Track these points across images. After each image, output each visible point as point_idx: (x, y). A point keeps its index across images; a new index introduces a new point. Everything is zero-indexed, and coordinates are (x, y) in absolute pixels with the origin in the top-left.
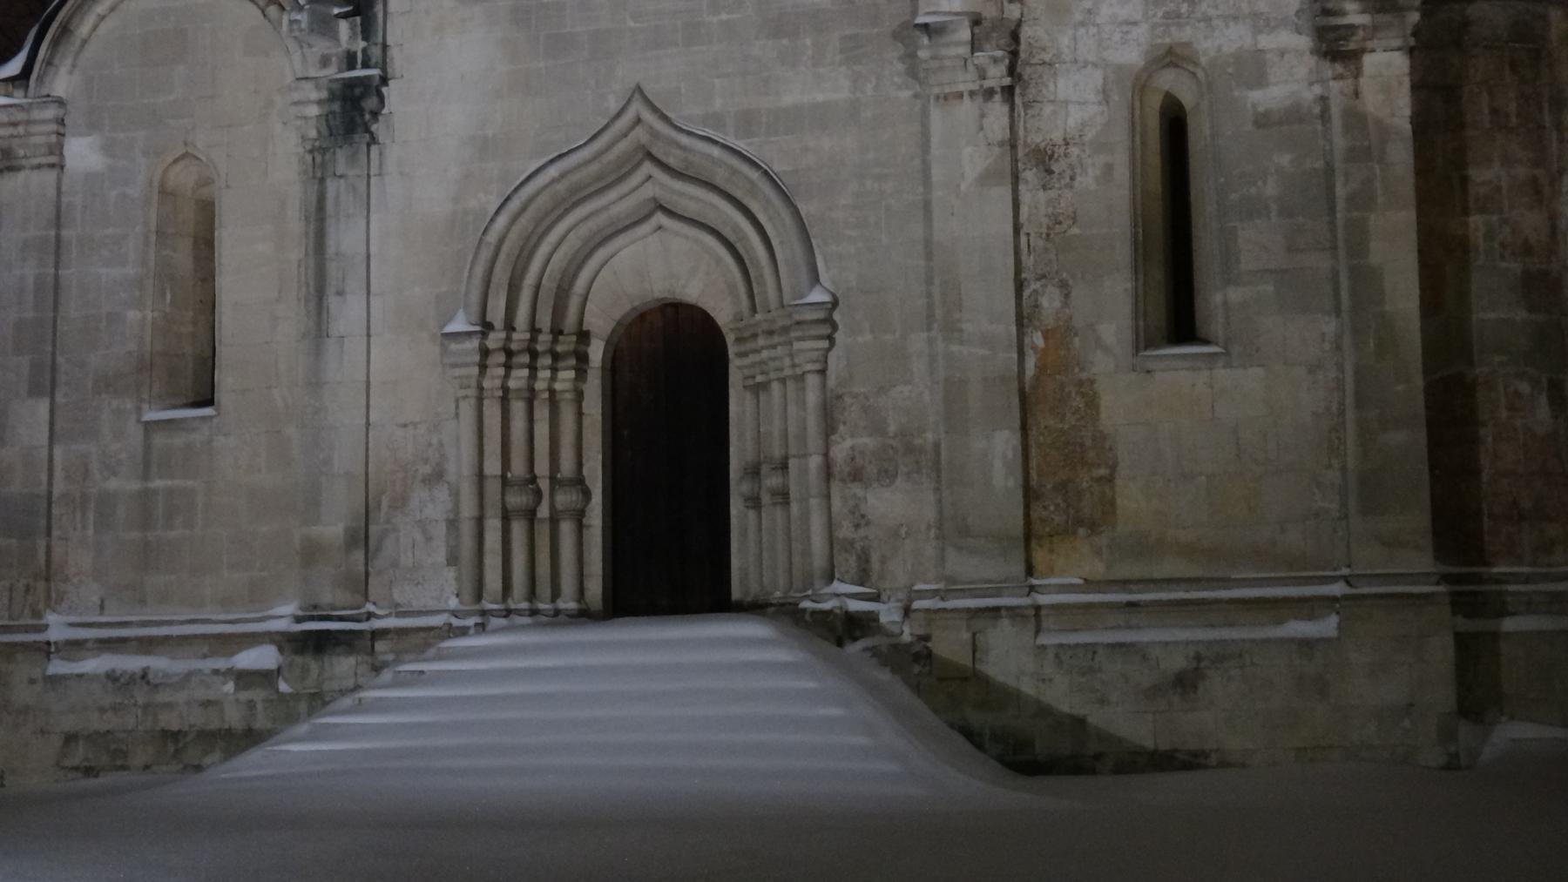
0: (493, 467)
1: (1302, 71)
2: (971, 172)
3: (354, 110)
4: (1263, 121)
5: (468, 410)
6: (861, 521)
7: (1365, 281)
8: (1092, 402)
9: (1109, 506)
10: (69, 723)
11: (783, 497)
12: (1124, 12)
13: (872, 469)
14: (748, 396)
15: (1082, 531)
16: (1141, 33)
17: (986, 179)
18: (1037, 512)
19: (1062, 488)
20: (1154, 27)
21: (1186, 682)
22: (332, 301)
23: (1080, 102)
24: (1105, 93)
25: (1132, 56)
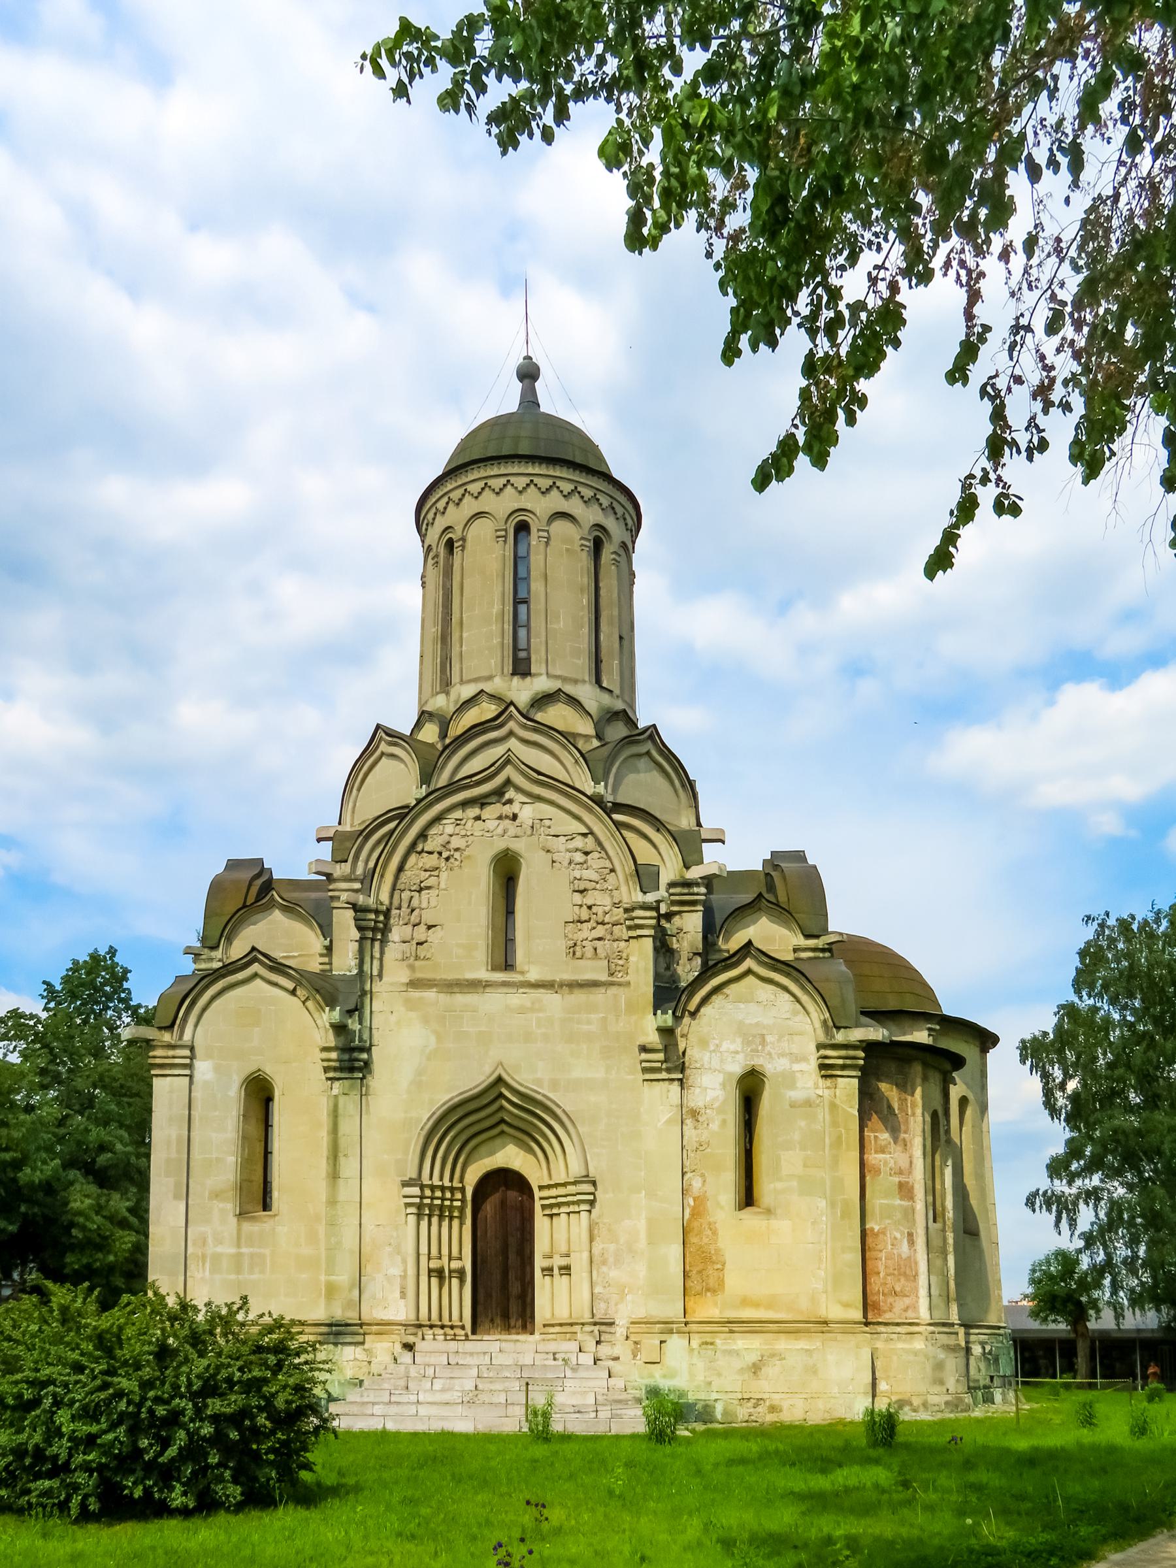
0: (424, 1249)
1: (811, 1084)
3: (352, 1060)
8: (715, 1233)
12: (732, 1047)
13: (611, 1260)
15: (709, 1294)
16: (740, 1057)
17: (669, 1121)
18: (689, 1284)
19: (700, 1272)
20: (746, 1056)
23: (714, 1088)
24: (724, 1085)
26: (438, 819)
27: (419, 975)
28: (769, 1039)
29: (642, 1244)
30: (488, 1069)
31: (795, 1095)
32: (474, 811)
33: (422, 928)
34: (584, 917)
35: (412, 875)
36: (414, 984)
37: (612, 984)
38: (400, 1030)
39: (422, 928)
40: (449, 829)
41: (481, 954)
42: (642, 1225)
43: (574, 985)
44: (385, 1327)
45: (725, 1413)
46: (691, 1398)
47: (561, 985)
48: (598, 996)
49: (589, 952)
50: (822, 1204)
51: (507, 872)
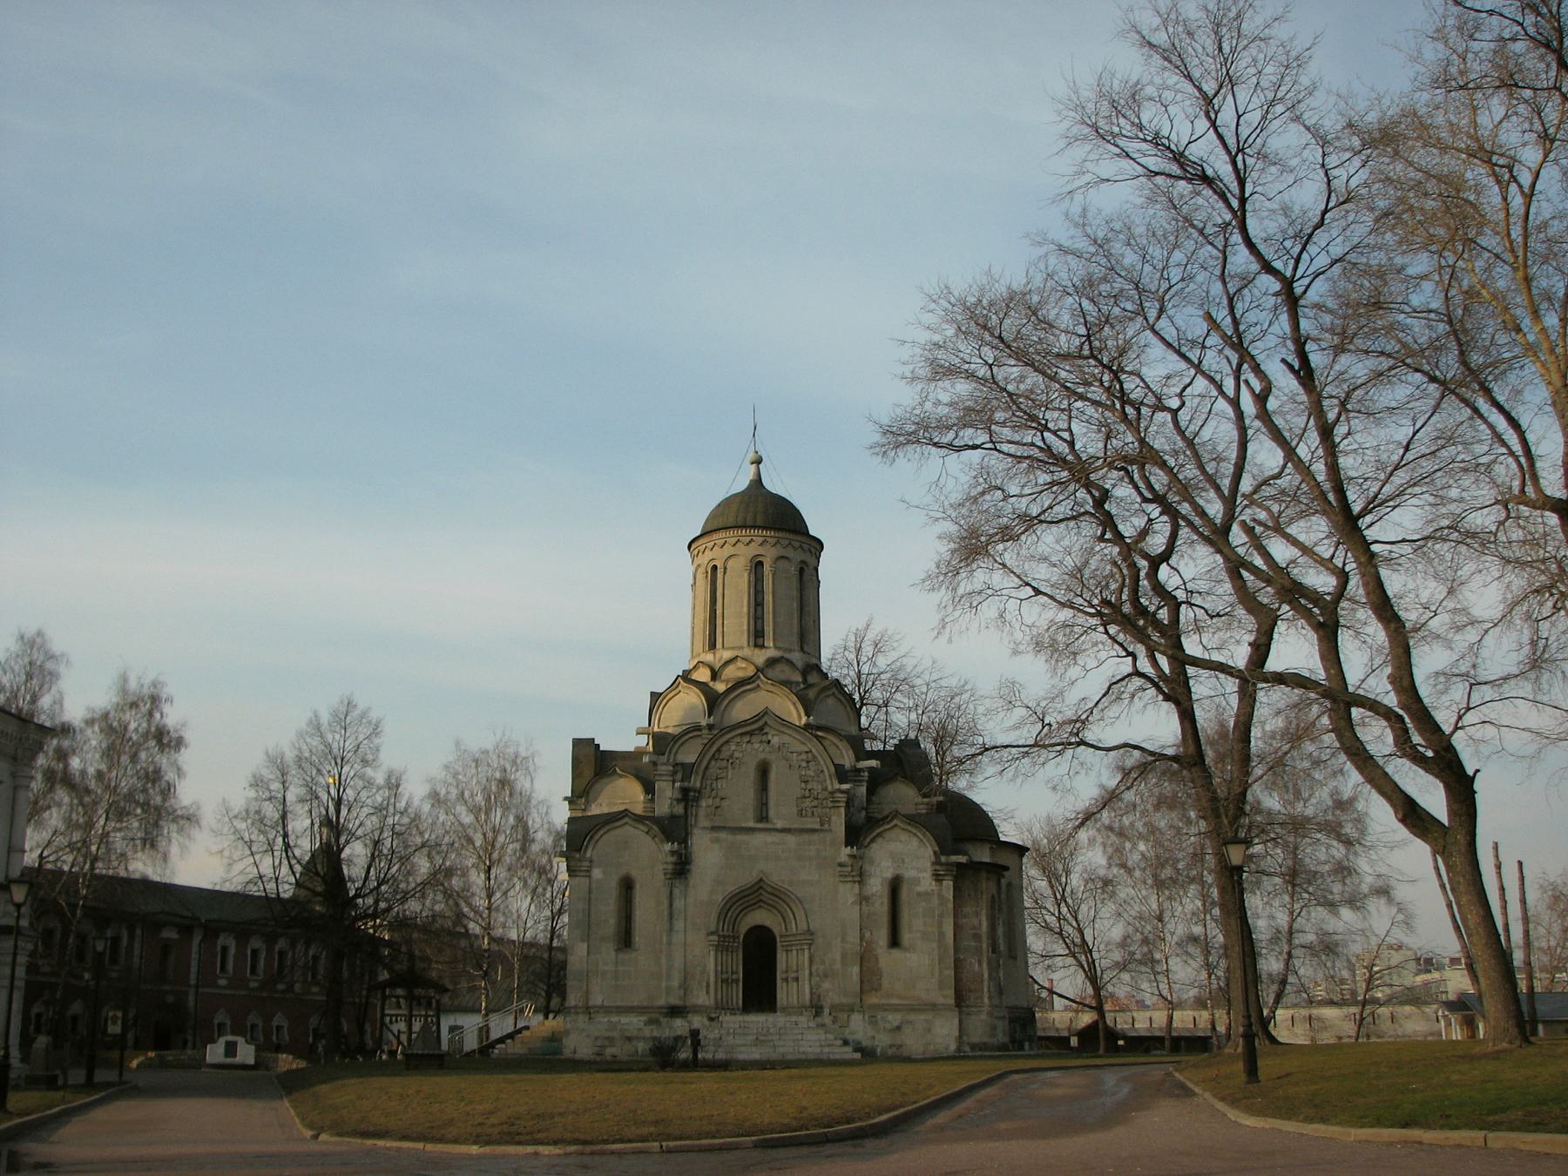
4: (919, 894)
7: (942, 935)
11: (797, 979)
21: (898, 1028)
23: (877, 885)
25: (889, 875)
29: (838, 965)
31: (919, 889)
32: (746, 739)
35: (713, 770)
36: (714, 828)
38: (707, 852)
41: (750, 814)
42: (838, 957)
43: (802, 831)
48: (815, 837)
50: (935, 945)
51: (764, 771)
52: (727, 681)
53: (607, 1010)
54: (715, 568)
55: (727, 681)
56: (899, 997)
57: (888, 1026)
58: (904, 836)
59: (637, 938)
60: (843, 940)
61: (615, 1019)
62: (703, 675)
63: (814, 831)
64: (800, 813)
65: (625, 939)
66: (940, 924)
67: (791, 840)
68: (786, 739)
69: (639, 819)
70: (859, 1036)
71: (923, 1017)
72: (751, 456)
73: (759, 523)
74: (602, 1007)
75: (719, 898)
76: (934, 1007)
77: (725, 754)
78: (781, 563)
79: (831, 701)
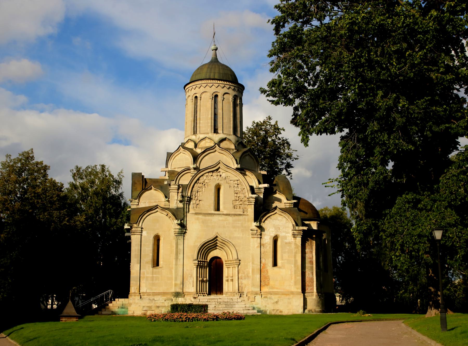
2: (256, 246)
4: (286, 243)
5: (195, 269)
6: (242, 284)
7: (296, 261)
8: (267, 272)
9: (269, 283)
10: (144, 305)
11: (232, 280)
14: (227, 269)
16: (274, 232)
17: (257, 247)
21: (277, 302)
22: (178, 254)
23: (268, 239)
24: (270, 239)
25: (273, 235)
26: (202, 175)
27: (197, 212)
28: (281, 228)
29: (251, 274)
30: (214, 234)
31: (287, 241)
32: (211, 174)
33: (198, 201)
34: (237, 199)
36: (196, 214)
37: (244, 215)
39: (198, 201)
40: (205, 178)
44: (189, 293)
45: (269, 312)
46: (262, 309)
47: (232, 215)
48: (241, 217)
49: (238, 207)
50: (293, 266)
52: (202, 148)
53: (149, 294)
54: (196, 97)
55: (202, 148)
56: (277, 288)
57: (273, 302)
58: (280, 218)
59: (161, 262)
60: (253, 263)
61: (151, 297)
62: (191, 145)
63: (240, 215)
64: (234, 207)
65: (156, 263)
66: (295, 257)
67: (230, 218)
68: (228, 174)
69: (164, 209)
70: (259, 306)
71: (288, 297)
72: (213, 47)
73: (216, 77)
74: (146, 293)
75: (199, 245)
76: (292, 293)
77: (201, 180)
78: (225, 96)
79: (247, 158)
